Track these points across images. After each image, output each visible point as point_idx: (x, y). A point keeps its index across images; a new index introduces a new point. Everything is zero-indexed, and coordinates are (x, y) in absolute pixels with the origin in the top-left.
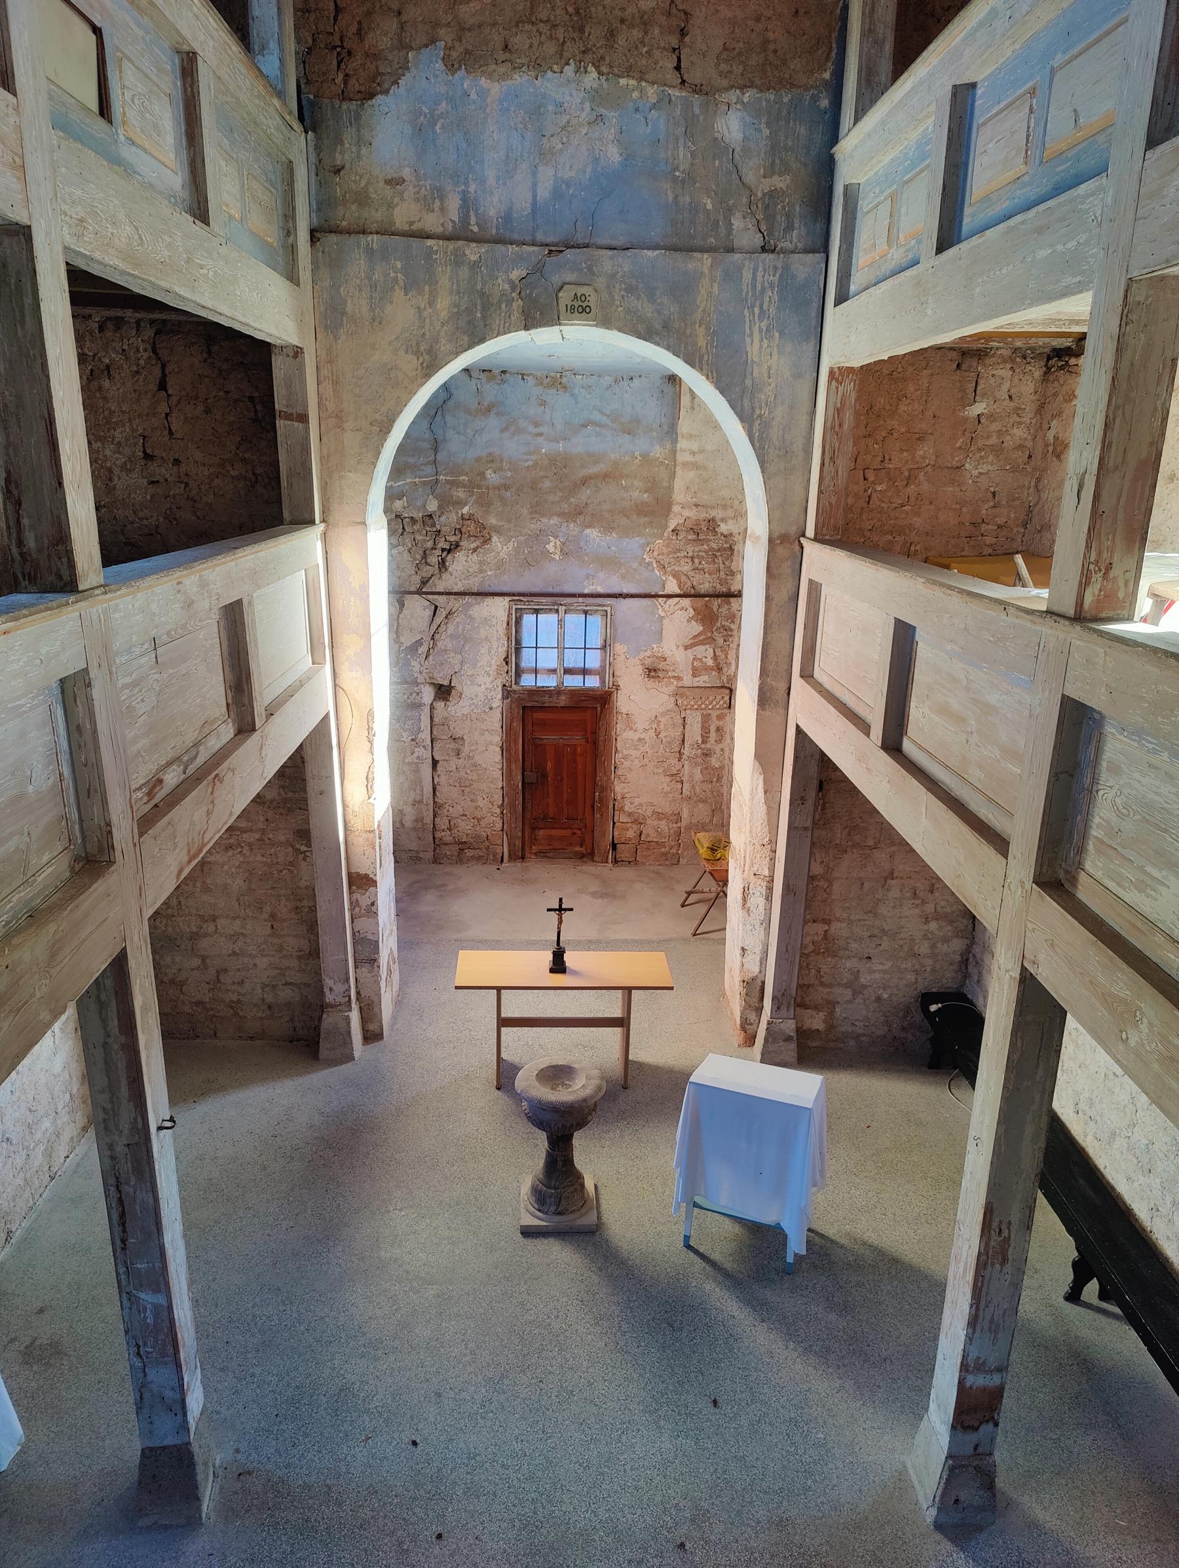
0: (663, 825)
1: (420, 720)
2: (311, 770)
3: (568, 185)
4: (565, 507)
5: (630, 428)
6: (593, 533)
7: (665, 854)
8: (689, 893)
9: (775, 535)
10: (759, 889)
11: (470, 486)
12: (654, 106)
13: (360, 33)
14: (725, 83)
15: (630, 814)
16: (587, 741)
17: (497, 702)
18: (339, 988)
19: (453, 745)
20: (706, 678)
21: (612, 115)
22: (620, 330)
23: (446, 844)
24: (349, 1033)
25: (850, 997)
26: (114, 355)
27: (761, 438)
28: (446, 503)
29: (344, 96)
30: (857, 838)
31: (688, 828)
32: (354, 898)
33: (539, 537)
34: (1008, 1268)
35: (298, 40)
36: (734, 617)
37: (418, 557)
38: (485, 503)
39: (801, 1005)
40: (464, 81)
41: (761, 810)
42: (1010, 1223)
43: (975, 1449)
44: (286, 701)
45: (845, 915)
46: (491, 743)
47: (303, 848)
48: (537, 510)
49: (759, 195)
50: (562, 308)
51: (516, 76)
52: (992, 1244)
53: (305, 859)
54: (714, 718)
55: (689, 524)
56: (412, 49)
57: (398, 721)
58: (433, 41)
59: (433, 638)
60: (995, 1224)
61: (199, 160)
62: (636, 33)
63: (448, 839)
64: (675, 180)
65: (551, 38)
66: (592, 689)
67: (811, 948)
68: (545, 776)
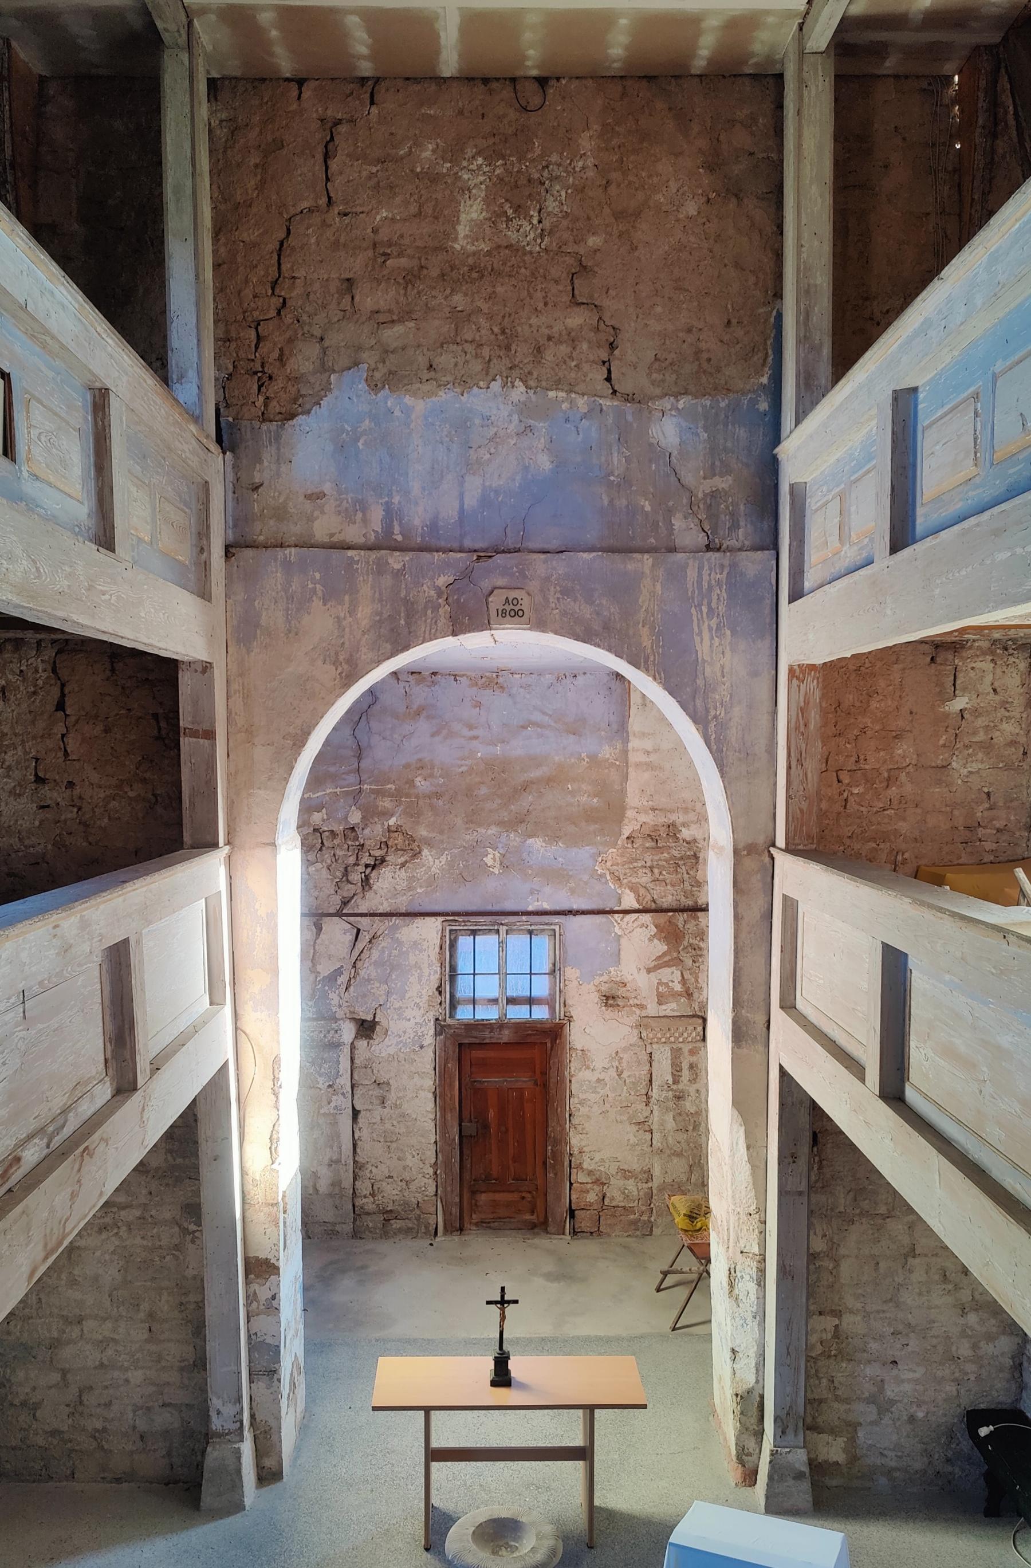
0: (631, 1185)
2: (204, 1131)
3: (497, 492)
4: (505, 815)
5: (575, 728)
6: (536, 844)
7: (635, 1223)
8: (665, 1274)
9: (741, 846)
10: (748, 1269)
11: (397, 796)
12: (584, 416)
13: (281, 359)
14: (658, 391)
15: (590, 1173)
17: (429, 1038)
18: (229, 1410)
19: (377, 1092)
20: (674, 1005)
21: (541, 426)
23: (368, 1214)
24: (239, 1471)
27: (718, 740)
28: (370, 814)
29: (264, 418)
30: (865, 1205)
31: (661, 1189)
32: (251, 1290)
33: (476, 849)
35: (219, 368)
36: (702, 935)
37: (339, 874)
38: (414, 814)
39: (812, 1427)
40: (387, 398)
41: (744, 1171)
44: (175, 1052)
45: (859, 1306)
46: (421, 1088)
47: (195, 1228)
48: (473, 819)
49: (700, 495)
51: (441, 393)
53: (193, 1242)
54: (686, 1053)
55: (646, 831)
56: (334, 371)
57: (313, 1063)
58: (356, 364)
59: (354, 967)
61: (106, 490)
62: (564, 349)
63: (371, 1207)
65: (477, 356)
66: (540, 1022)
67: (819, 1349)
68: (486, 1126)
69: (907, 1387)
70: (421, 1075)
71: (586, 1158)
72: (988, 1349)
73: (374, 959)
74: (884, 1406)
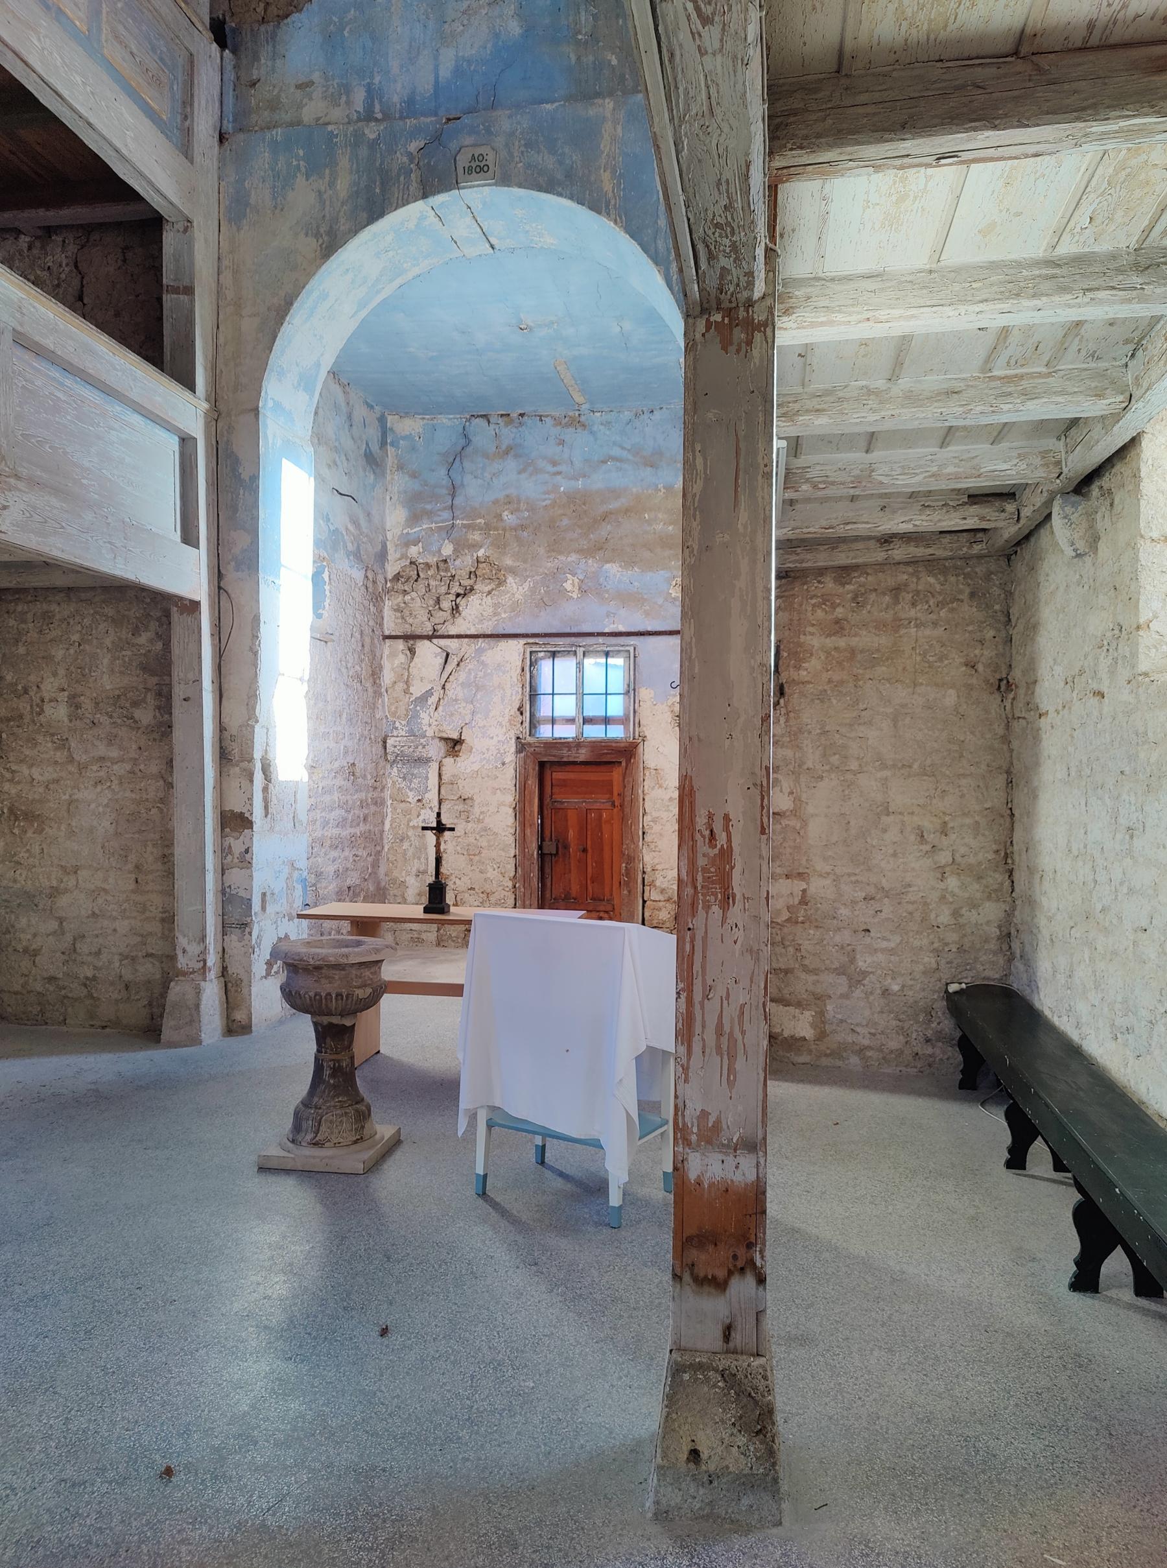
1: (427, 778)
3: (469, 62)
6: (612, 569)
15: (663, 891)
16: (614, 805)
17: (510, 756)
19: (461, 807)
22: (520, 186)
25: (844, 989)
26: (39, 272)
30: (835, 760)
32: (226, 844)
33: (556, 575)
34: (736, 912)
37: (431, 602)
38: (500, 545)
42: (727, 818)
43: (727, 1337)
45: (828, 869)
46: (502, 804)
48: (555, 548)
50: (460, 171)
52: (701, 862)
59: (443, 687)
60: (701, 821)
64: (578, 42)
67: (786, 915)
68: (566, 847)
69: (880, 957)
70: (503, 790)
71: (658, 875)
72: (971, 916)
73: (461, 680)
74: (856, 979)
